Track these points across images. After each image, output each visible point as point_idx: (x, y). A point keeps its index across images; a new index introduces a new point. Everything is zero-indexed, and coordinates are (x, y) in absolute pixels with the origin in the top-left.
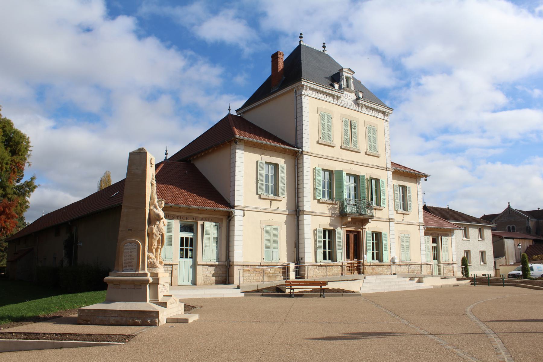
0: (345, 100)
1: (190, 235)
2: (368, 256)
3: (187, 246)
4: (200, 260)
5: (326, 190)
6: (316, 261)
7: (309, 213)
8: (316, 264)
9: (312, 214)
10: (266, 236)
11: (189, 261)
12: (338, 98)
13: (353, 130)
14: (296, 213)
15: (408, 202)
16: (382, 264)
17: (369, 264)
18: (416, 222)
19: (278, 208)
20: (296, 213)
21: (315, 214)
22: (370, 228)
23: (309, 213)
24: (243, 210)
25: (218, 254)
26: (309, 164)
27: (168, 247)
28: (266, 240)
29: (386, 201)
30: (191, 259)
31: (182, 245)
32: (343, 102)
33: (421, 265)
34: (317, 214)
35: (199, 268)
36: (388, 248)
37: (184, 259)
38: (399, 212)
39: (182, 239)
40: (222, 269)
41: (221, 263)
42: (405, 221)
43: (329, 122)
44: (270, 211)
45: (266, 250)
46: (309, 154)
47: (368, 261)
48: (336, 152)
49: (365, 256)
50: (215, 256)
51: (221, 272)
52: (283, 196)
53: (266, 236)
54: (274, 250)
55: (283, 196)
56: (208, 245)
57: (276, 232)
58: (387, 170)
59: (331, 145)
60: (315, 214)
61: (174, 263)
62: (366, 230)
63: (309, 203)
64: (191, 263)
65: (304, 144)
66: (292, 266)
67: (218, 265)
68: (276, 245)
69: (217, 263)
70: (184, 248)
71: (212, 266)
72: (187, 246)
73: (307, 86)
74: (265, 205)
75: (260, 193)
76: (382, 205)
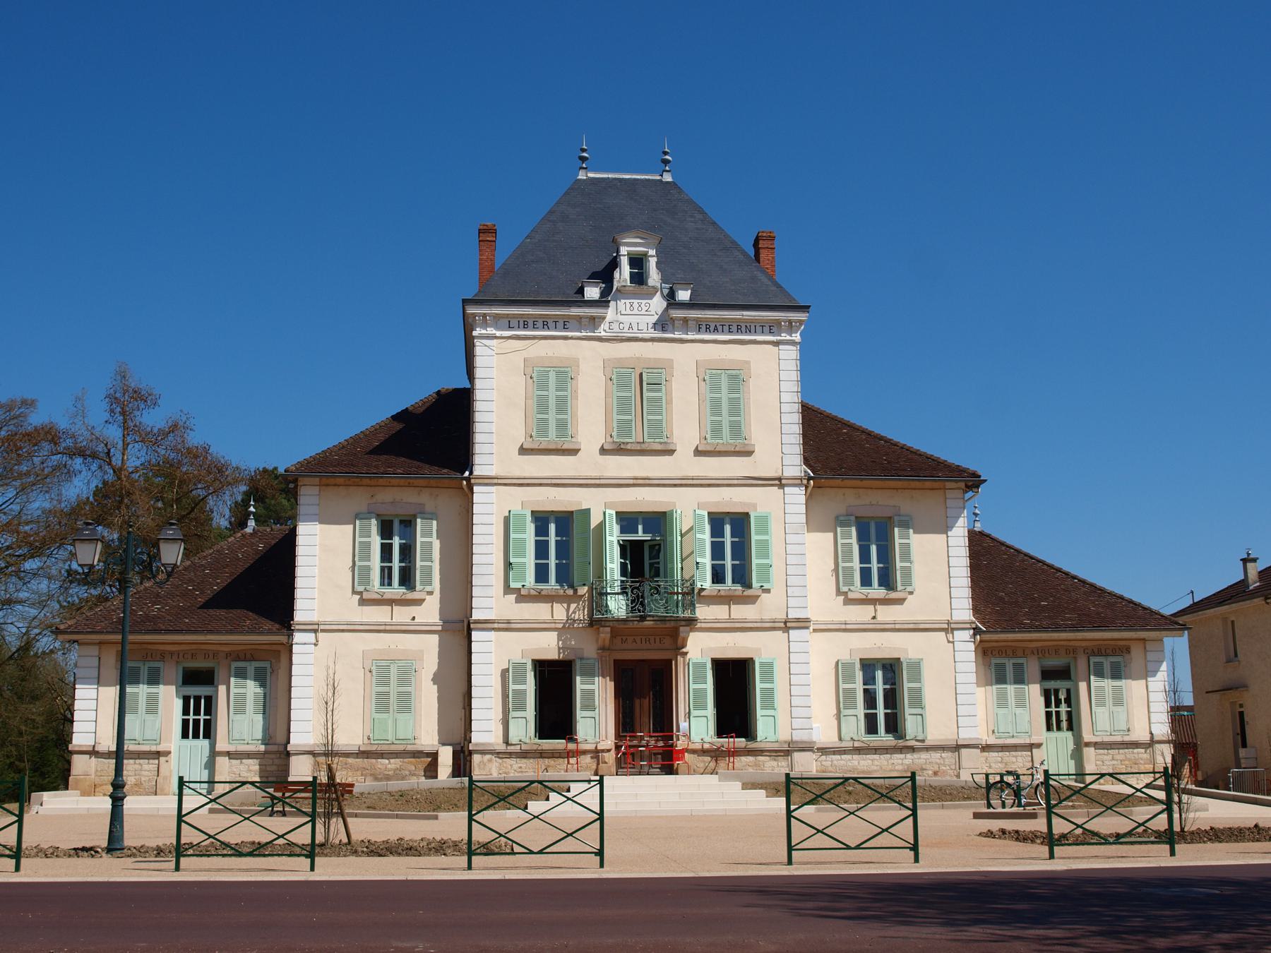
0: (622, 318)
1: (202, 691)
2: (697, 723)
3: (197, 712)
4: (221, 745)
5: (552, 561)
6: (507, 742)
7: (487, 625)
8: (502, 747)
9: (496, 626)
10: (378, 684)
11: (204, 743)
12: (594, 322)
13: (646, 394)
14: (459, 629)
15: (899, 564)
16: (752, 745)
17: (698, 746)
18: (942, 616)
19: (414, 618)
20: (459, 629)
21: (507, 626)
22: (701, 649)
23: (487, 625)
24: (315, 631)
25: (266, 729)
26: (490, 508)
27: (150, 717)
28: (378, 694)
29: (776, 574)
30: (206, 742)
31: (186, 711)
32: (615, 327)
33: (957, 748)
34: (513, 626)
35: (222, 762)
36: (780, 699)
37: (191, 742)
38: (851, 595)
39: (186, 700)
40: (277, 761)
41: (274, 748)
42: (880, 618)
43: (561, 386)
44: (388, 628)
45: (377, 716)
46: (490, 481)
47: (696, 737)
48: (589, 462)
49: (684, 725)
50: (259, 734)
51: (274, 768)
52: (428, 588)
53: (378, 684)
54: (401, 717)
55: (428, 588)
56: (241, 710)
57: (406, 676)
58: (782, 486)
59: (565, 447)
60: (507, 626)
61: (160, 748)
62: (689, 656)
63: (489, 600)
64: (206, 752)
65: (477, 459)
66: (446, 757)
67: (266, 752)
68: (405, 703)
69: (262, 748)
70: (191, 717)
71: (249, 755)
72: (197, 712)
73: (484, 316)
74: (378, 615)
75: (361, 589)
76: (755, 584)
